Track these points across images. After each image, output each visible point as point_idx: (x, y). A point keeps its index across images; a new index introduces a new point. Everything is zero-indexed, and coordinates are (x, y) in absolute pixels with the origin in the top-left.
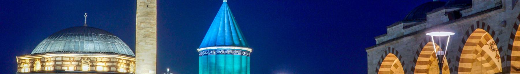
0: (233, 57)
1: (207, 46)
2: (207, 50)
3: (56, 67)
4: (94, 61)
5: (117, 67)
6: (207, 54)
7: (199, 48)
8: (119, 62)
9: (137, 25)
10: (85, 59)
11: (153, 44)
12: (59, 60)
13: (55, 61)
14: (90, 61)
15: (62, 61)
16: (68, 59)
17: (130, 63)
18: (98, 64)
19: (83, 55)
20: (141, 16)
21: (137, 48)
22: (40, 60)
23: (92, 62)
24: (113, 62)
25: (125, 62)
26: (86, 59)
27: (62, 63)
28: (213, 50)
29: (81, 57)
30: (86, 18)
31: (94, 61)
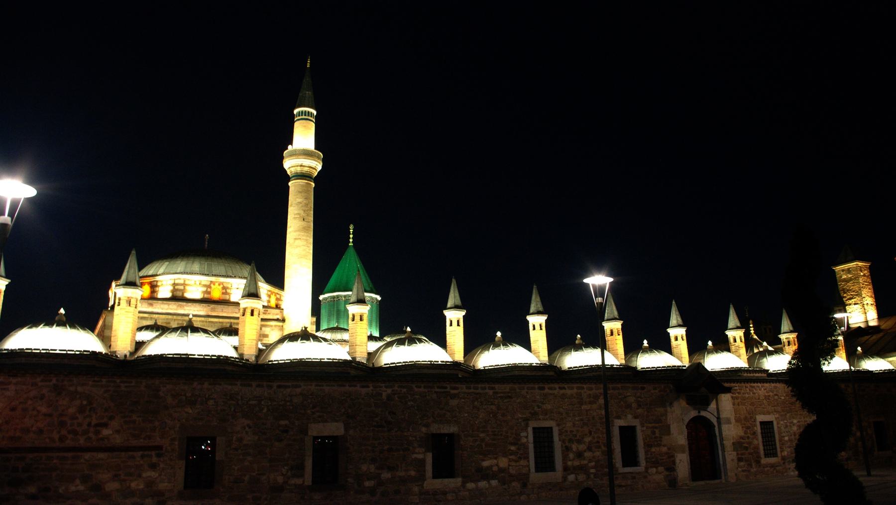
2: (334, 296)
3: (175, 293)
9: (289, 243)
13: (174, 284)
15: (184, 285)
19: (213, 279)
20: (295, 231)
23: (224, 288)
26: (217, 284)
27: (184, 287)
28: (341, 296)
29: (211, 282)
30: (207, 240)
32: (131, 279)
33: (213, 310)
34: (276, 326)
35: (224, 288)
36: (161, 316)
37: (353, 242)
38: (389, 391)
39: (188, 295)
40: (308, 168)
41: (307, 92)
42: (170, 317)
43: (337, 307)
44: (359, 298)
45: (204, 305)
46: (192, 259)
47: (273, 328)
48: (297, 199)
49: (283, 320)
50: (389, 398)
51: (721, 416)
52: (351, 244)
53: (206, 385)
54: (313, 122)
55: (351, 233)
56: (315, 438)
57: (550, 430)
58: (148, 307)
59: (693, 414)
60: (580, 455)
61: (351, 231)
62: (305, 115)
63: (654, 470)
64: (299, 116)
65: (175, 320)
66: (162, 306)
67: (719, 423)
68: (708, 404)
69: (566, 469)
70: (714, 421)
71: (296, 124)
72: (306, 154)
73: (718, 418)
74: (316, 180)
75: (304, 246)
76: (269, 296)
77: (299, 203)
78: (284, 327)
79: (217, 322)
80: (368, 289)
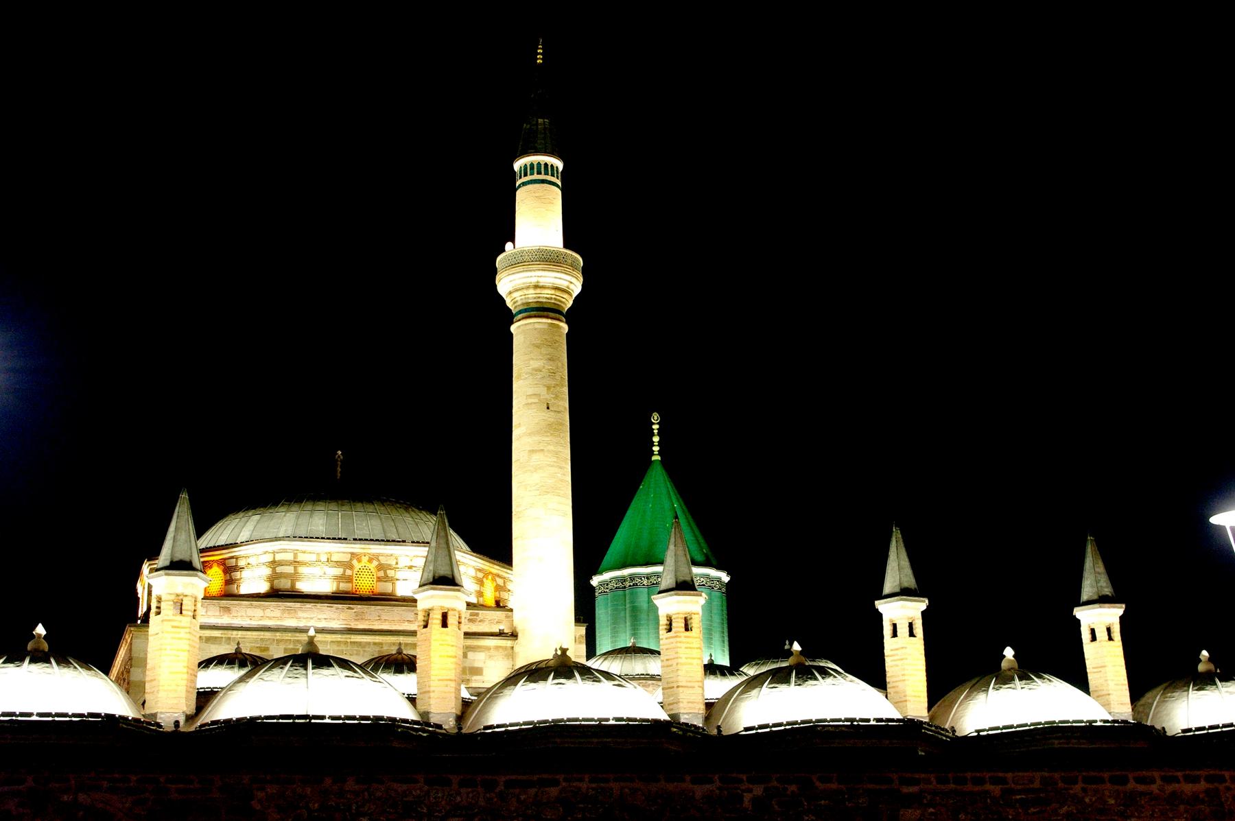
1: (624, 566)
3: (276, 582)
4: (389, 567)
6: (625, 587)
10: (363, 557)
12: (286, 561)
13: (274, 564)
14: (377, 567)
17: (484, 577)
18: (399, 575)
19: (357, 548)
20: (530, 434)
22: (224, 564)
23: (381, 567)
25: (472, 572)
26: (365, 559)
27: (295, 568)
28: (640, 576)
29: (352, 554)
31: (390, 565)
32: (179, 556)
33: (360, 616)
34: (497, 648)
36: (249, 633)
37: (660, 453)
38: (758, 790)
39: (304, 587)
40: (553, 292)
41: (540, 121)
42: (268, 635)
43: (632, 602)
44: (681, 578)
45: (340, 606)
48: (531, 362)
49: (514, 635)
52: (656, 458)
53: (351, 785)
54: (558, 186)
55: (656, 431)
61: (656, 427)
62: (539, 173)
64: (526, 175)
65: (279, 641)
66: (251, 612)
71: (521, 195)
72: (547, 259)
74: (571, 316)
75: (552, 466)
76: (480, 582)
77: (533, 369)
78: (517, 649)
80: (699, 558)
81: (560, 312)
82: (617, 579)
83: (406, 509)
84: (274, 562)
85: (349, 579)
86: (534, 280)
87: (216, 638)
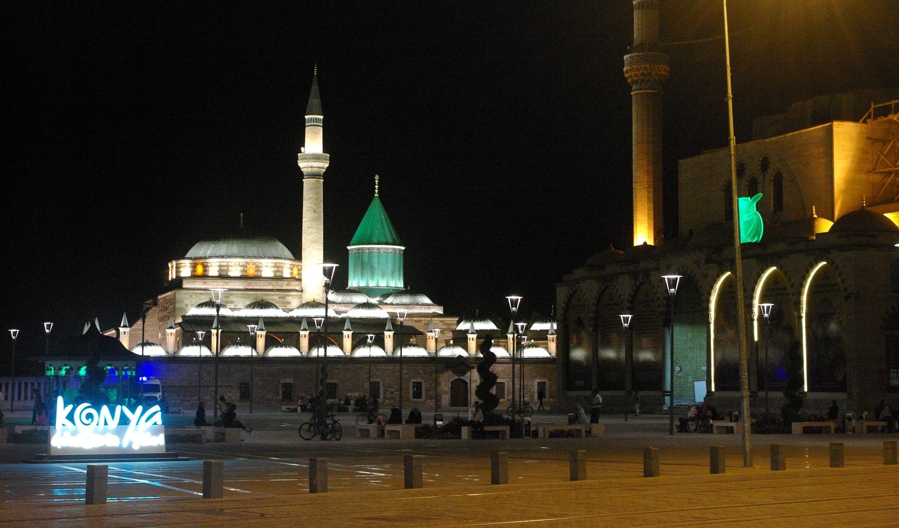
0: (387, 256)
4: (260, 267)
5: (282, 272)
7: (349, 245)
8: (284, 267)
11: (320, 250)
13: (220, 266)
16: (234, 264)
19: (248, 260)
20: (308, 221)
21: (305, 254)
23: (257, 267)
24: (279, 267)
25: (289, 266)
26: (251, 264)
28: (365, 249)
29: (247, 262)
30: (242, 218)
33: (249, 284)
34: (296, 295)
35: (257, 267)
38: (311, 367)
39: (231, 274)
41: (315, 100)
46: (232, 242)
47: (294, 297)
48: (310, 195)
49: (302, 291)
50: (310, 370)
51: (472, 379)
52: (376, 195)
55: (377, 183)
56: (283, 384)
57: (378, 383)
58: (203, 285)
59: (456, 377)
60: (392, 393)
62: (314, 122)
63: (430, 401)
66: (213, 283)
67: (470, 382)
68: (465, 374)
69: (385, 398)
70: (468, 381)
71: (307, 129)
72: (316, 157)
73: (470, 380)
76: (292, 269)
78: (303, 296)
79: (252, 294)
81: (320, 175)
82: (359, 249)
83: (266, 241)
84: (220, 265)
85: (246, 271)
86: (311, 165)
87: (202, 293)
